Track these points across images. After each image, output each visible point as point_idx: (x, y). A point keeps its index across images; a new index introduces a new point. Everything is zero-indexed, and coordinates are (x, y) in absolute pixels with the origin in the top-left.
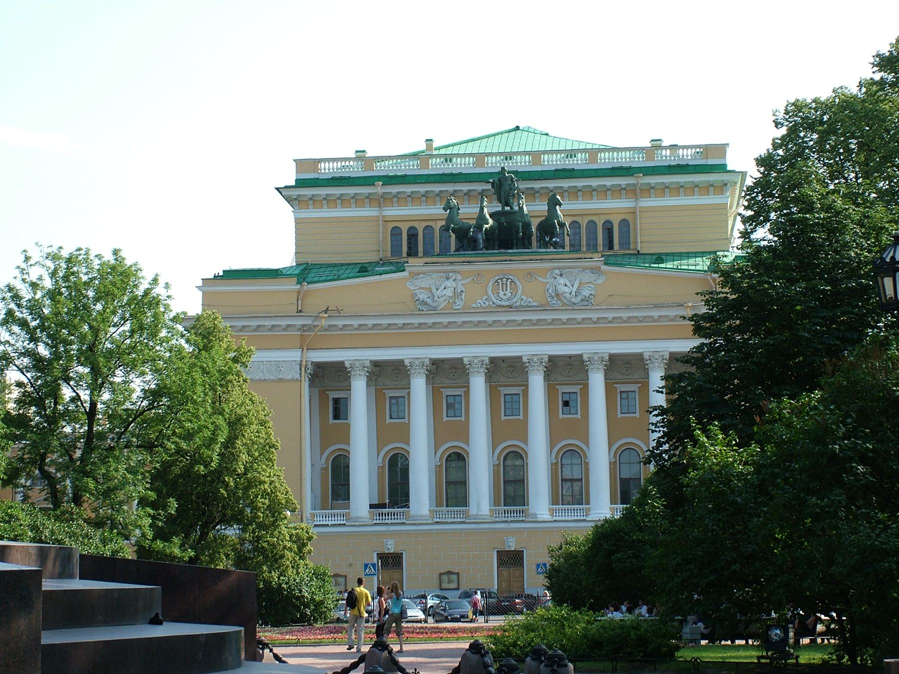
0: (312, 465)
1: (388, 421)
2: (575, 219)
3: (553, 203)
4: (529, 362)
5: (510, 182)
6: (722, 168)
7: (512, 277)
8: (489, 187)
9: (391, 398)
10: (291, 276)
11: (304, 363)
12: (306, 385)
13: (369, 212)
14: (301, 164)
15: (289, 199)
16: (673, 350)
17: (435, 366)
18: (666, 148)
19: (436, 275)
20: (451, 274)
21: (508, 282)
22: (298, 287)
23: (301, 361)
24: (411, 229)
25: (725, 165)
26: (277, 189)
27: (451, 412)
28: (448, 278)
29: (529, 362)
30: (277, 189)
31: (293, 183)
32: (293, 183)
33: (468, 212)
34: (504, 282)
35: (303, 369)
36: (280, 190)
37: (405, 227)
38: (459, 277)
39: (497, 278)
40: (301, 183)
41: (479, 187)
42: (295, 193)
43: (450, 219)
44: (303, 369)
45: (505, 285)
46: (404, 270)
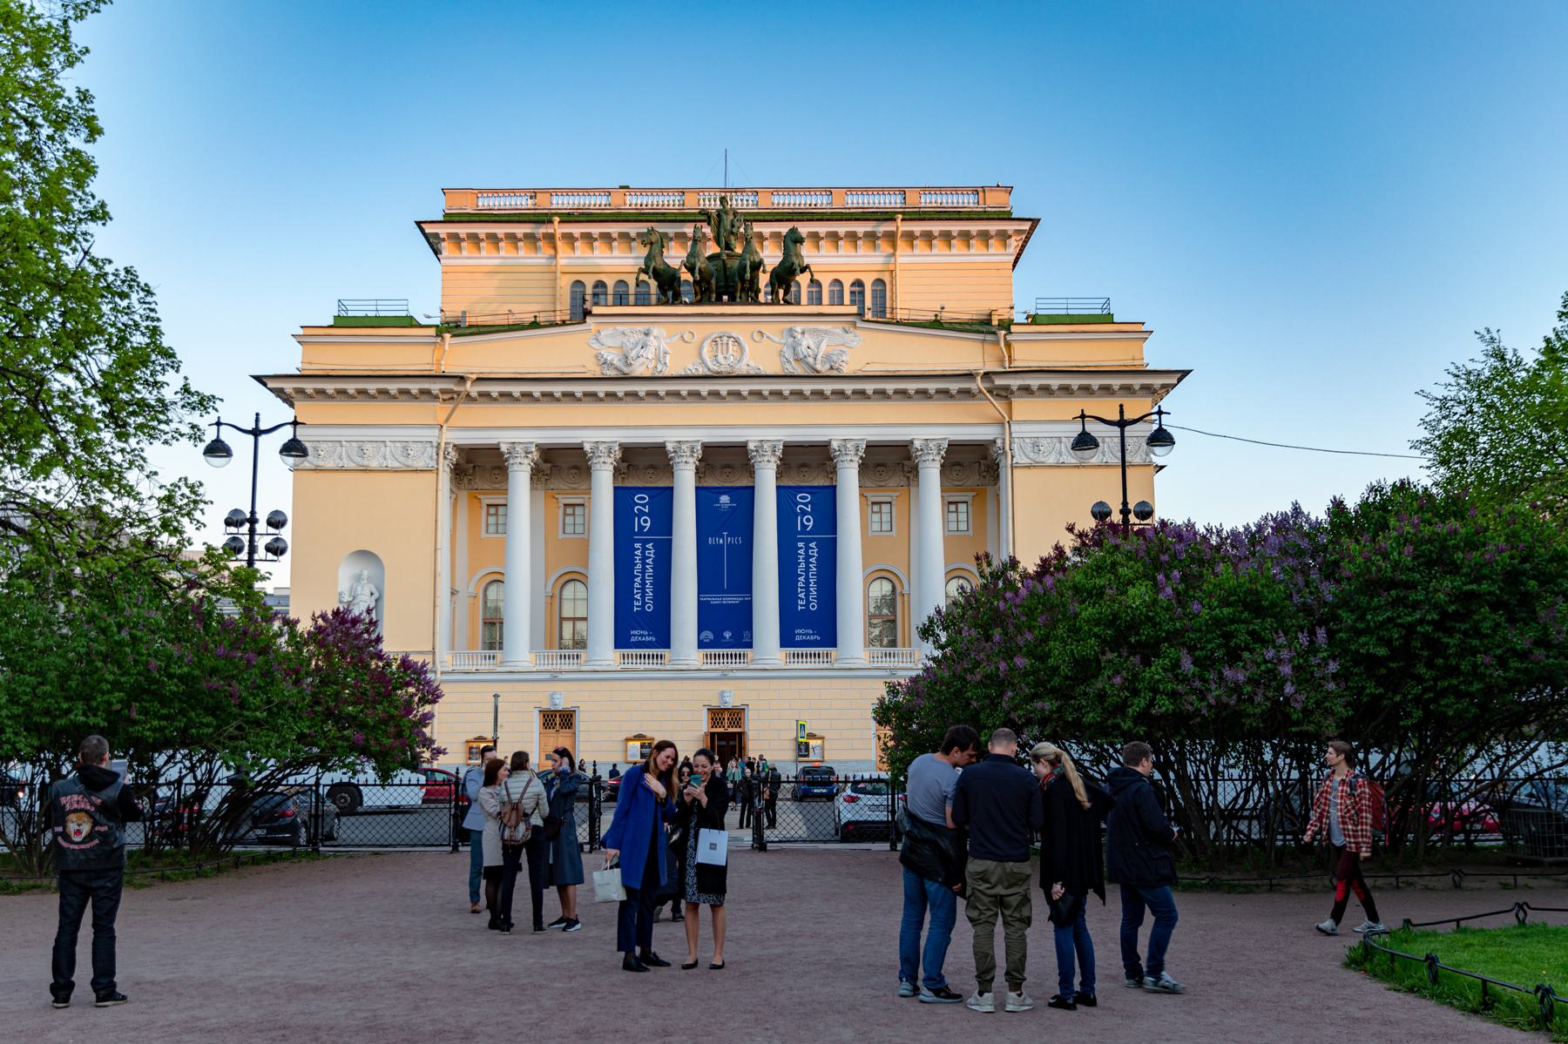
0: (453, 593)
3: (794, 239)
4: (757, 451)
5: (731, 217)
7: (733, 335)
11: (443, 445)
12: (445, 477)
15: (434, 243)
16: (952, 438)
17: (625, 464)
21: (730, 342)
23: (439, 444)
25: (1010, 213)
26: (419, 224)
29: (757, 451)
30: (419, 224)
33: (675, 257)
34: (725, 342)
35: (441, 453)
36: (423, 226)
39: (715, 336)
42: (443, 231)
44: (441, 453)
45: (725, 346)
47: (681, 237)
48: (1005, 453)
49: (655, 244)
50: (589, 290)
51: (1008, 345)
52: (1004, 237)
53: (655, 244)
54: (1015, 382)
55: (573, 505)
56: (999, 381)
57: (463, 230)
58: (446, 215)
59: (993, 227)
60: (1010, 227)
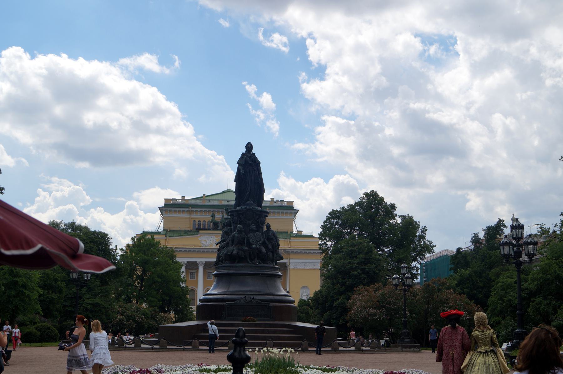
1: (207, 279)
2: (204, 220)
6: (291, 208)
8: (224, 210)
9: (191, 272)
10: (163, 235)
13: (186, 215)
14: (165, 199)
18: (275, 201)
19: (207, 236)
20: (212, 236)
22: (166, 238)
24: (199, 221)
25: (293, 207)
27: (209, 278)
28: (211, 237)
31: (163, 206)
32: (163, 206)
37: (197, 221)
38: (215, 237)
40: (166, 206)
41: (221, 210)
42: (164, 209)
43: (212, 220)
46: (198, 234)
47: (218, 212)
48: (288, 265)
49: (213, 216)
50: (197, 224)
51: (290, 242)
52: (291, 213)
53: (213, 216)
54: (290, 251)
55: (193, 272)
56: (287, 251)
57: (169, 209)
58: (165, 205)
59: (289, 211)
60: (293, 211)
